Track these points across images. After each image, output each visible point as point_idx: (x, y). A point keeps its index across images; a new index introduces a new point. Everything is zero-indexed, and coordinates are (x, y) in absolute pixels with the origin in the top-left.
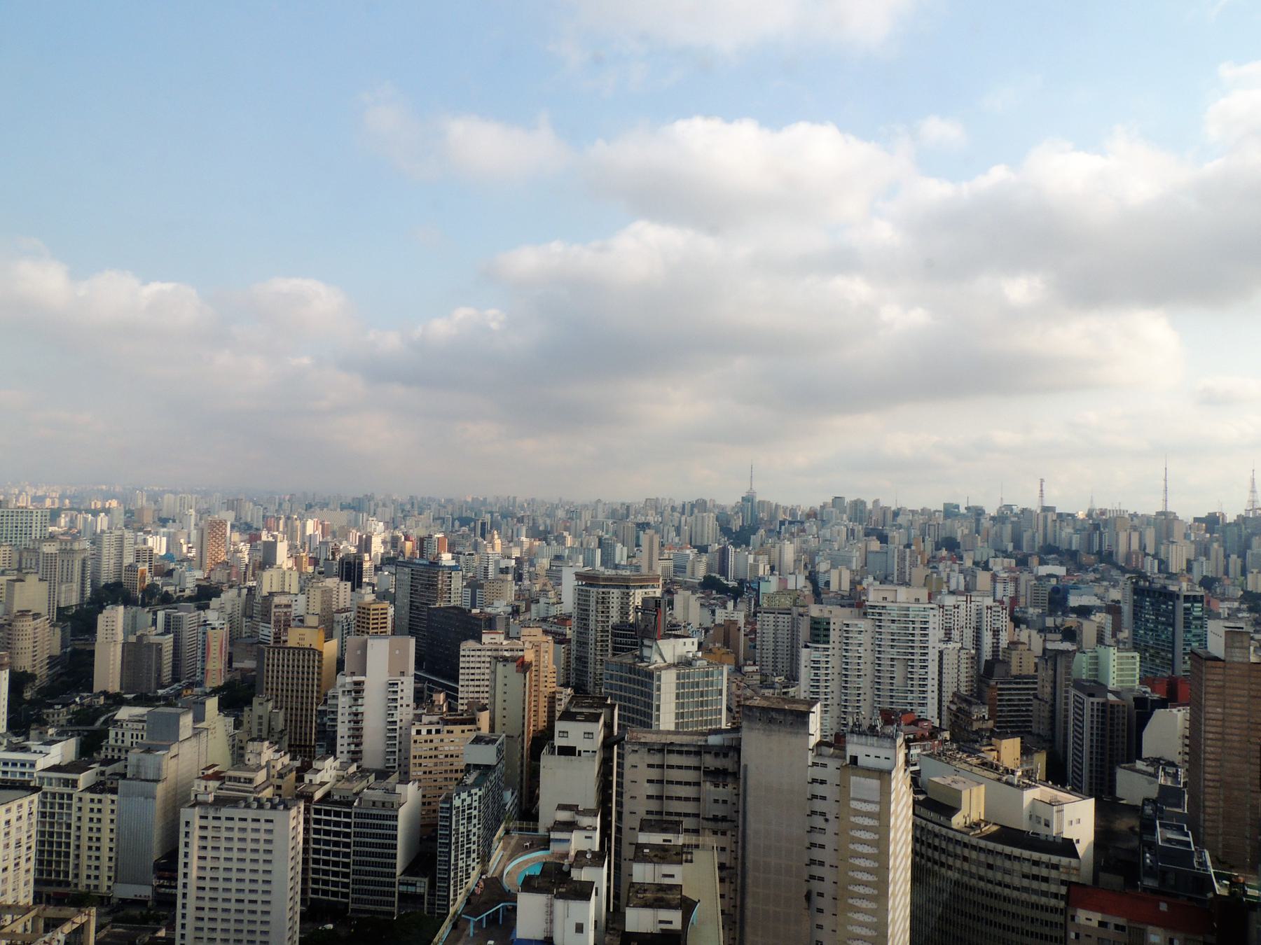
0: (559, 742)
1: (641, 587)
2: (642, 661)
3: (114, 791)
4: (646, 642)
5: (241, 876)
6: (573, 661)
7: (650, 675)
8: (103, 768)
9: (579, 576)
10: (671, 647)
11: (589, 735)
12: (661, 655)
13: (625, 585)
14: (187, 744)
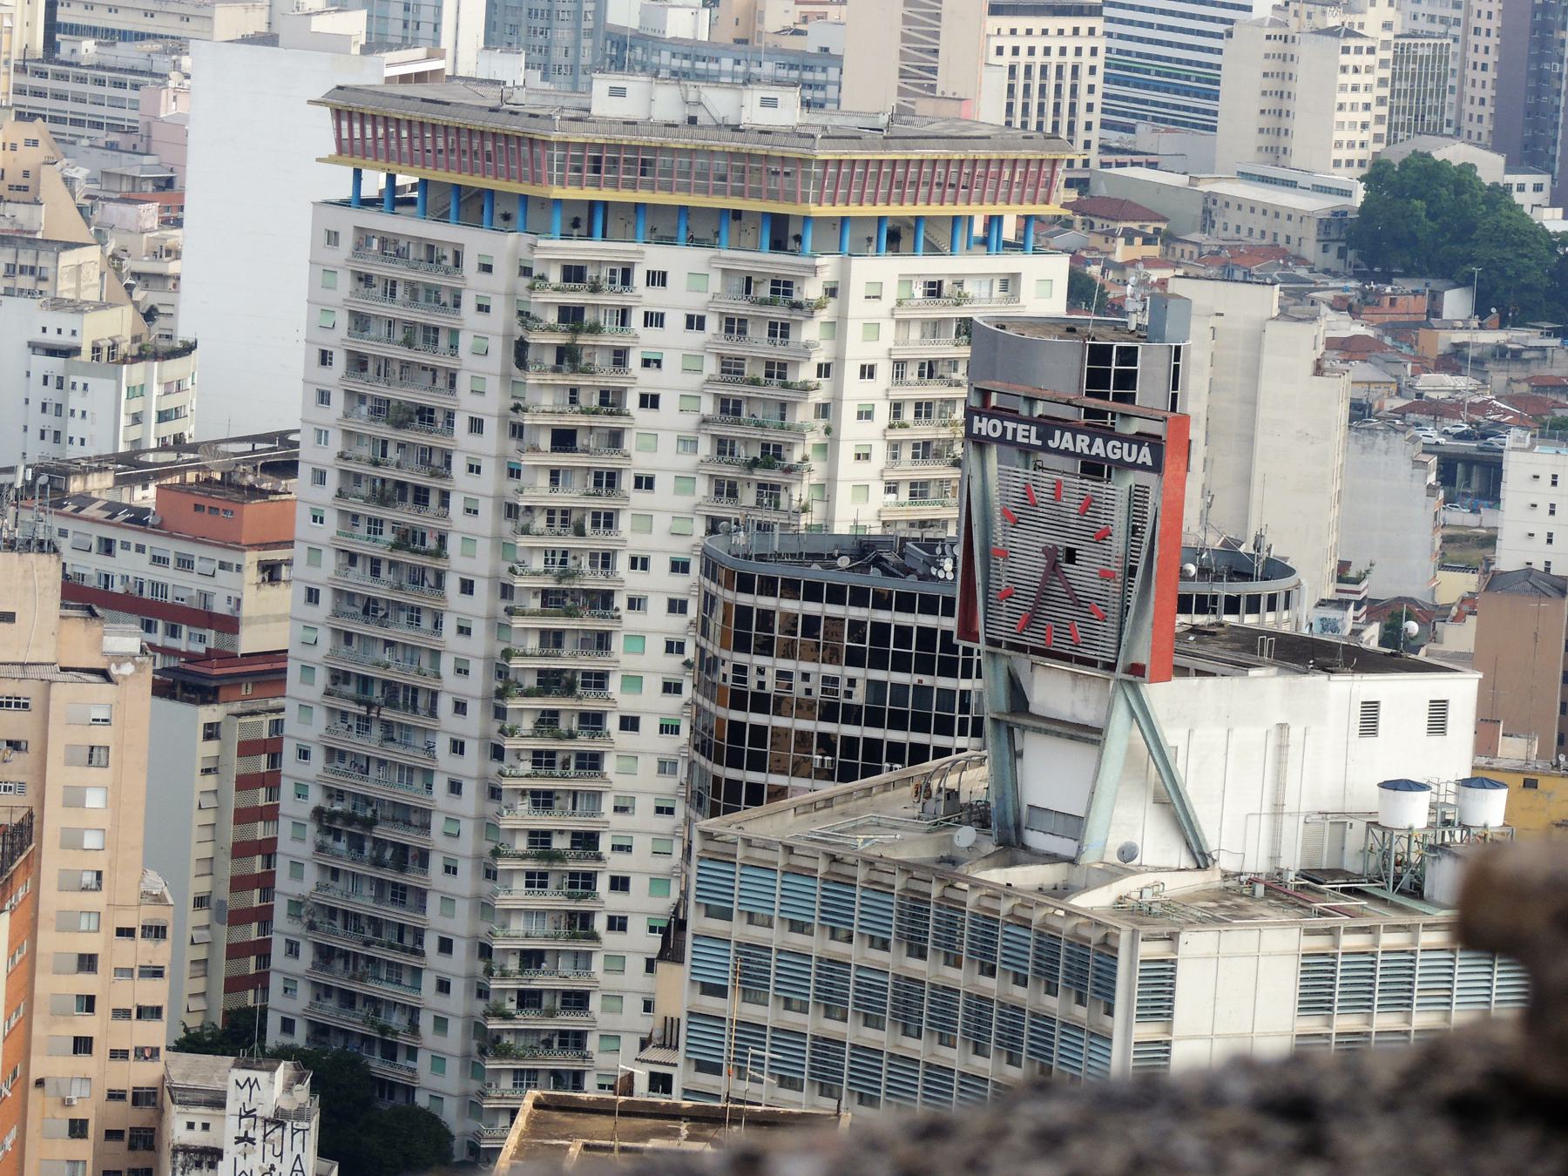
1: (895, 237)
2: (1012, 848)
4: (1053, 691)
6: (295, 844)
7: (1084, 966)
9: (362, 123)
10: (1253, 737)
12: (1173, 806)
13: (761, 210)
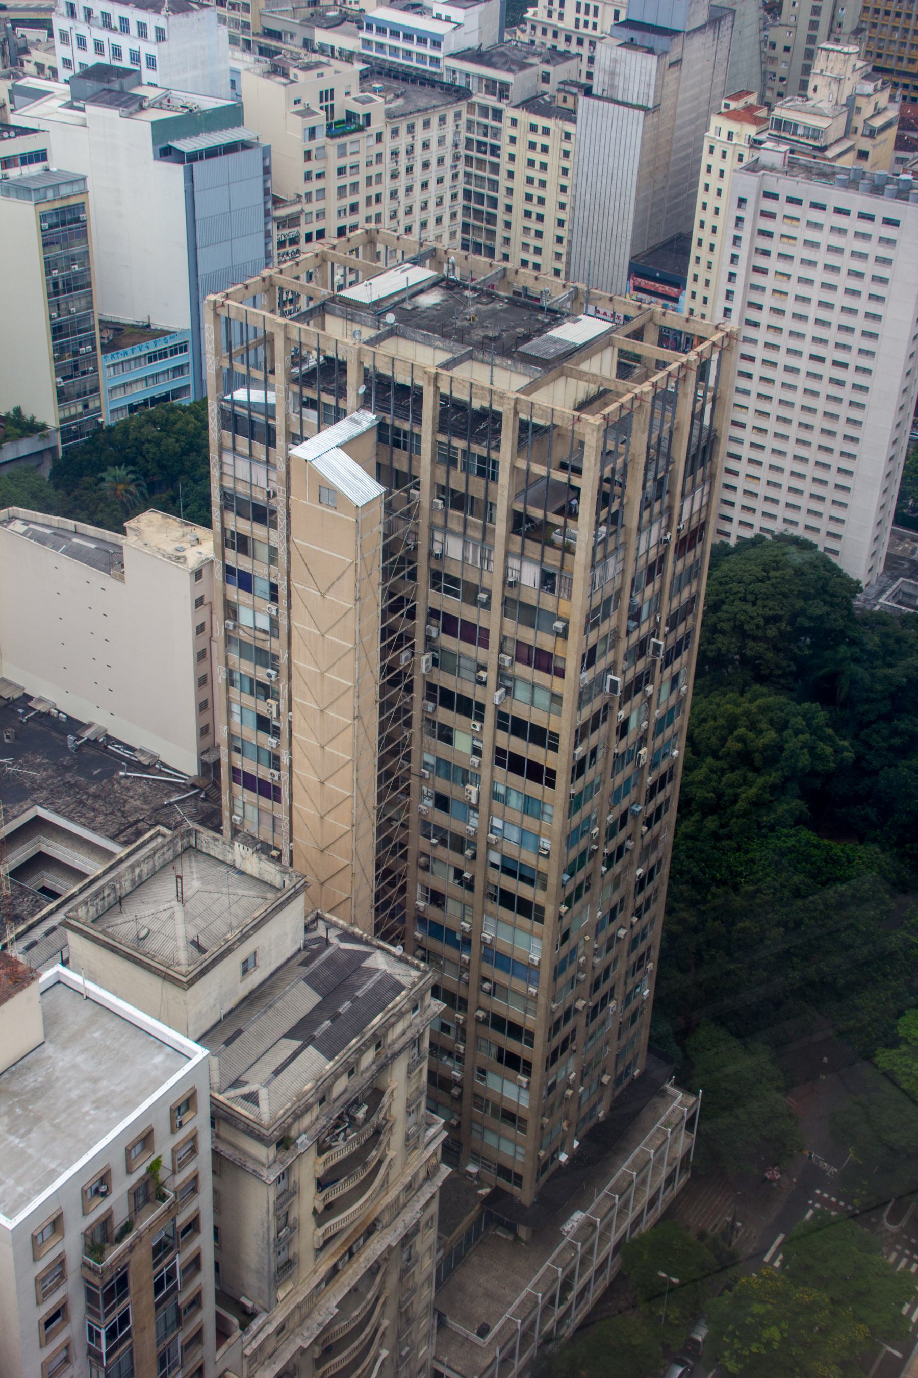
3: (570, 115)
5: (824, 314)
8: (548, 68)
14: (698, 40)
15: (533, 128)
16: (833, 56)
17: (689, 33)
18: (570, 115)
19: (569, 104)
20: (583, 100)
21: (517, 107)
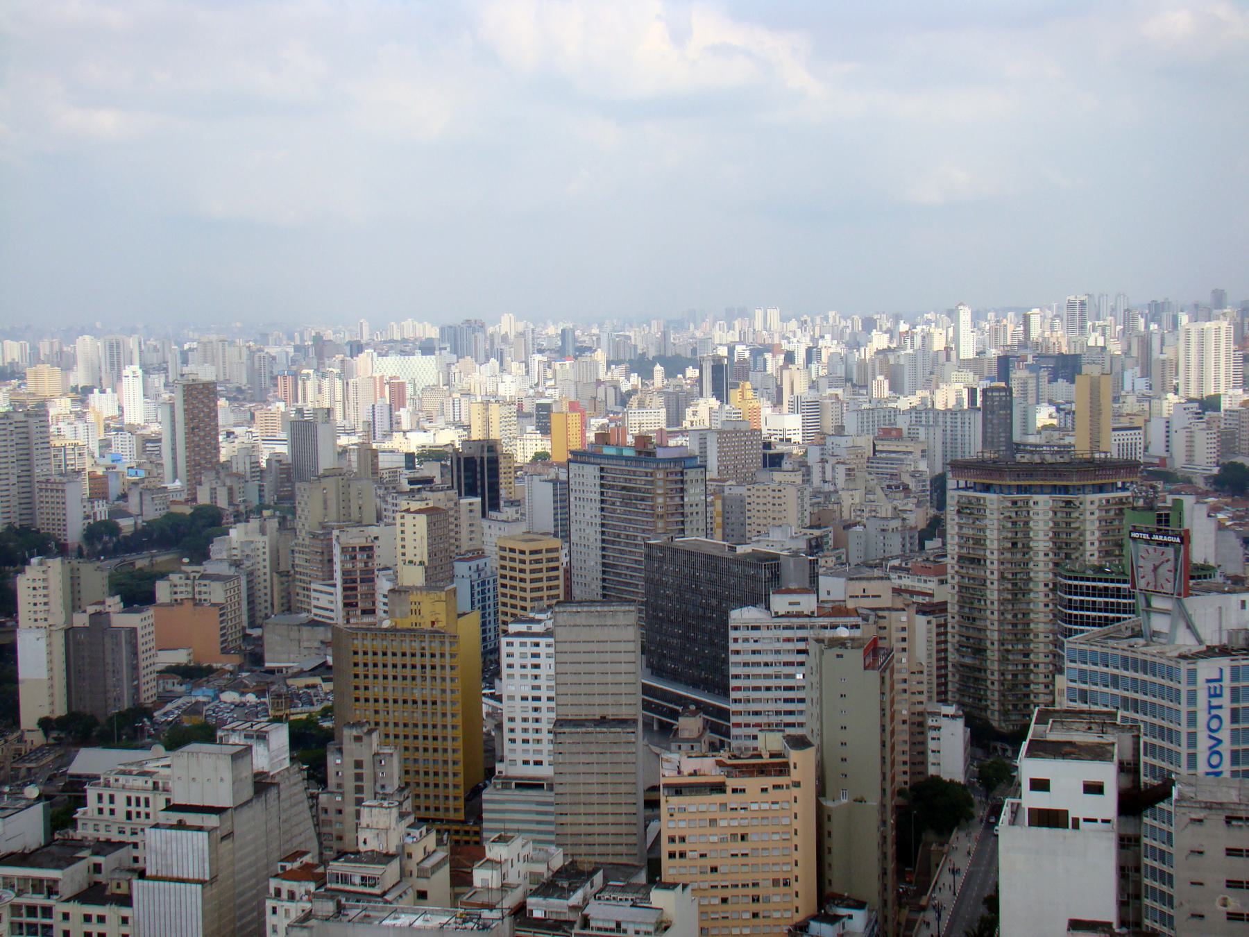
0: (1031, 800)
3: (126, 900)
11: (1094, 788)
14: (247, 813)
15: (88, 918)
16: (375, 811)
17: (236, 808)
18: (126, 900)
19: (123, 890)
20: (137, 884)
21: (68, 900)
